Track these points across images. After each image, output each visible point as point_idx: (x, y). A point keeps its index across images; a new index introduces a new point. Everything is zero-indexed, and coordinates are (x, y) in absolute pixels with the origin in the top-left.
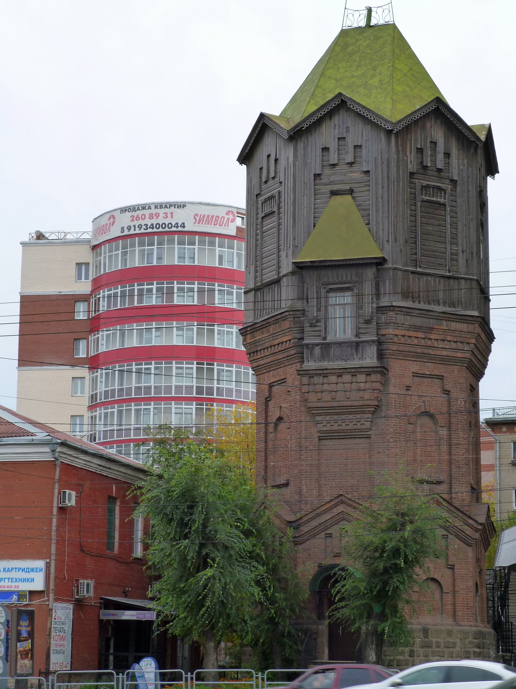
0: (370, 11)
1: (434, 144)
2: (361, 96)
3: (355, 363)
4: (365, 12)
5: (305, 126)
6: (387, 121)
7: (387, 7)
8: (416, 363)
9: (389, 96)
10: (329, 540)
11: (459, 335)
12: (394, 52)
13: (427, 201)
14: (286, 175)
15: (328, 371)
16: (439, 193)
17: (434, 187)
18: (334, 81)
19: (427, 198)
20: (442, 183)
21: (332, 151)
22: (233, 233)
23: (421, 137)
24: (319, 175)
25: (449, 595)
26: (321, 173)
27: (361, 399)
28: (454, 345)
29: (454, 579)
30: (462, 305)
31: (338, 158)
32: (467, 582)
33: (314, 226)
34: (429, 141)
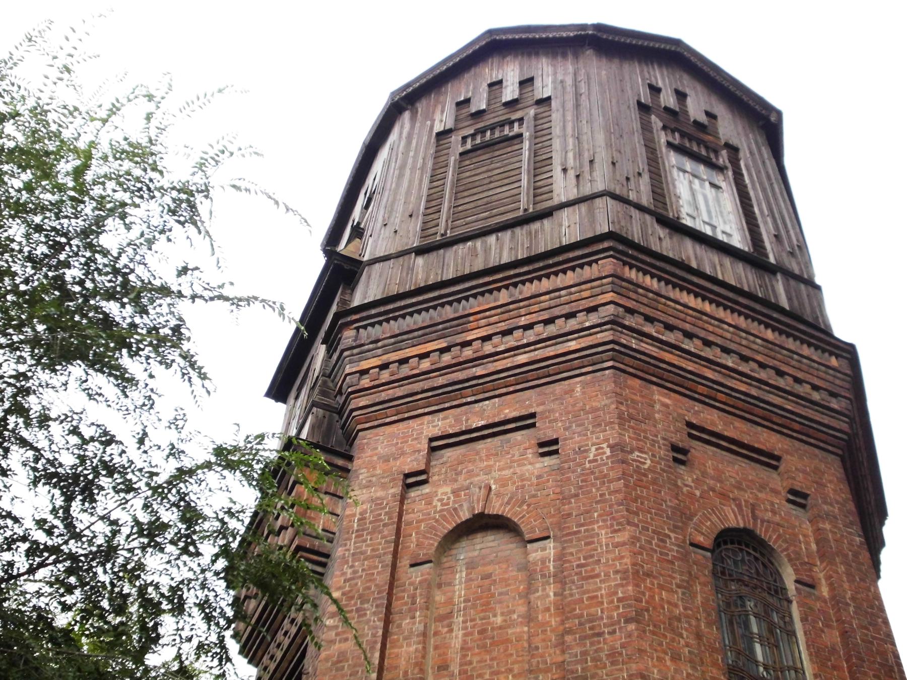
8: (441, 415)
11: (553, 303)
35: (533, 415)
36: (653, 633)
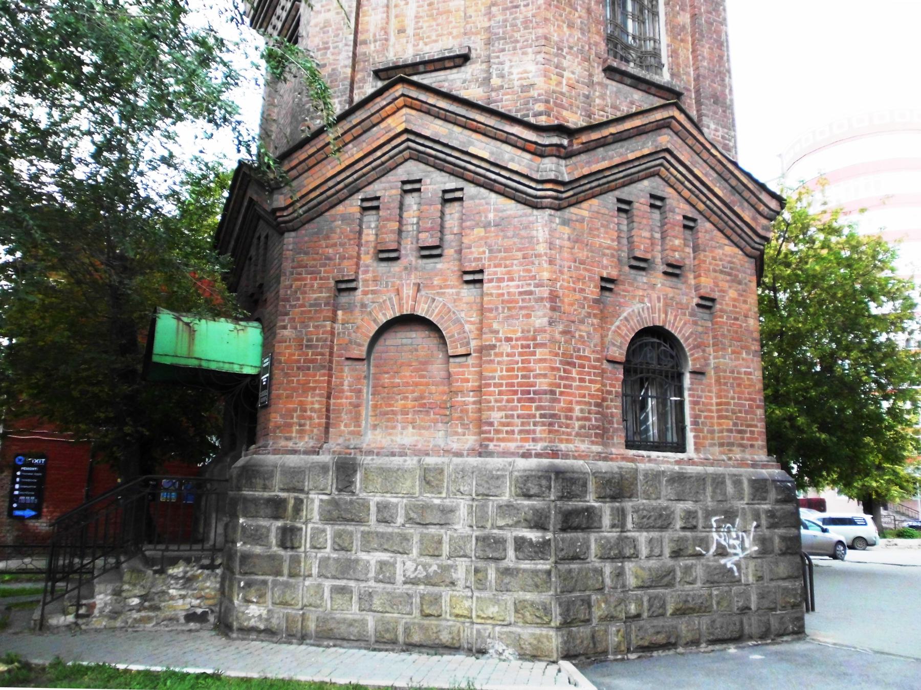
25: (470, 361)
29: (482, 310)
32: (528, 316)
36: (557, 7)
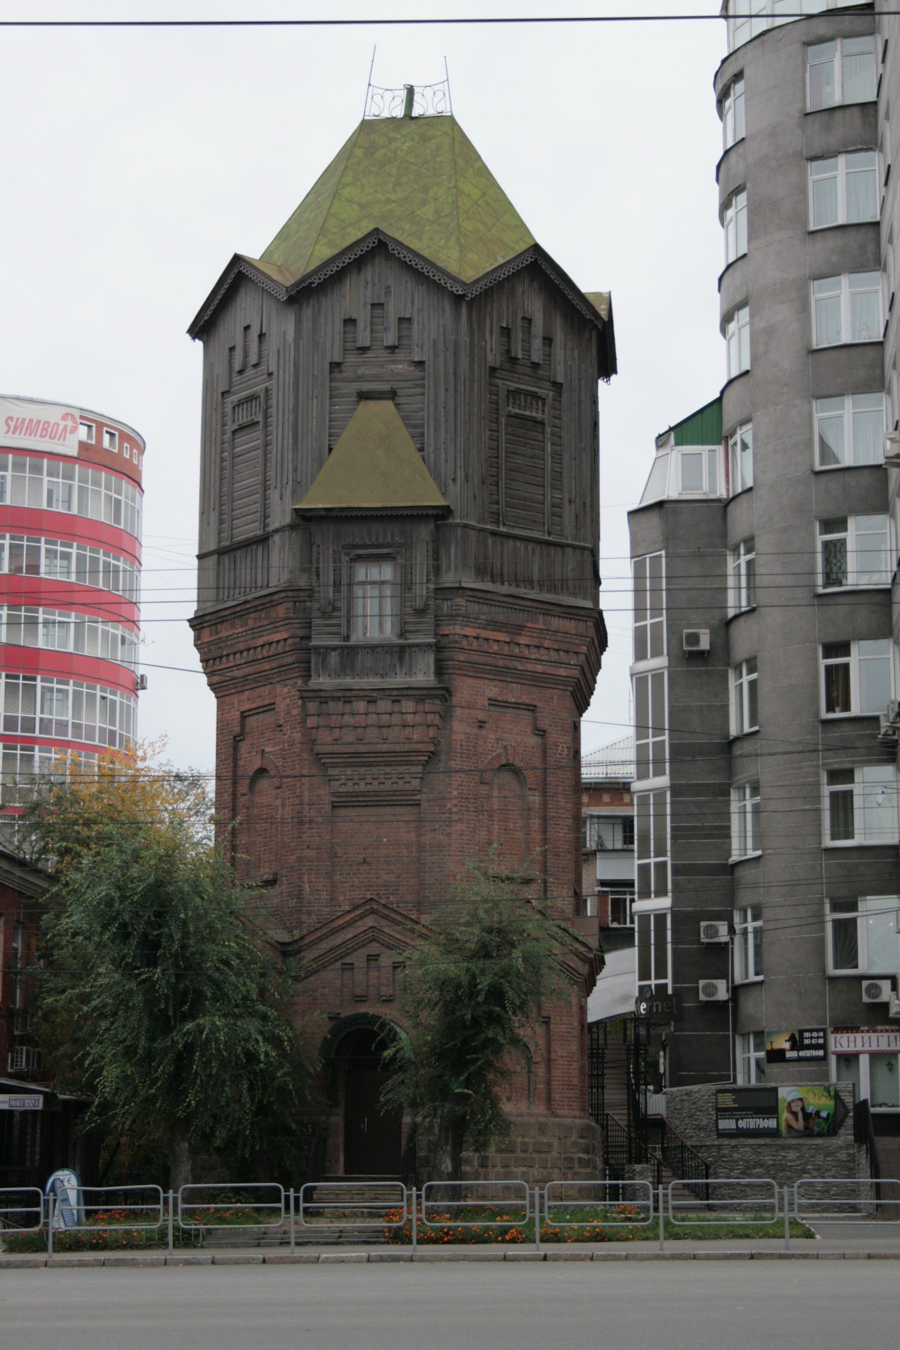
0: (410, 91)
1: (528, 321)
2: (405, 235)
3: (399, 680)
4: (403, 94)
5: (317, 281)
6: (455, 280)
7: (440, 87)
8: (494, 683)
9: (454, 238)
10: (348, 974)
12: (455, 164)
13: (516, 416)
14: (281, 362)
15: (353, 693)
16: (534, 403)
17: (528, 394)
18: (357, 208)
19: (516, 411)
20: (539, 388)
21: (361, 325)
22: (73, 451)
23: (508, 309)
24: (339, 364)
26: (341, 361)
27: (407, 741)
28: (554, 656)
30: (568, 589)
31: (372, 337)
32: (569, 1045)
33: (330, 450)
34: (519, 318)
35: (535, 706)
